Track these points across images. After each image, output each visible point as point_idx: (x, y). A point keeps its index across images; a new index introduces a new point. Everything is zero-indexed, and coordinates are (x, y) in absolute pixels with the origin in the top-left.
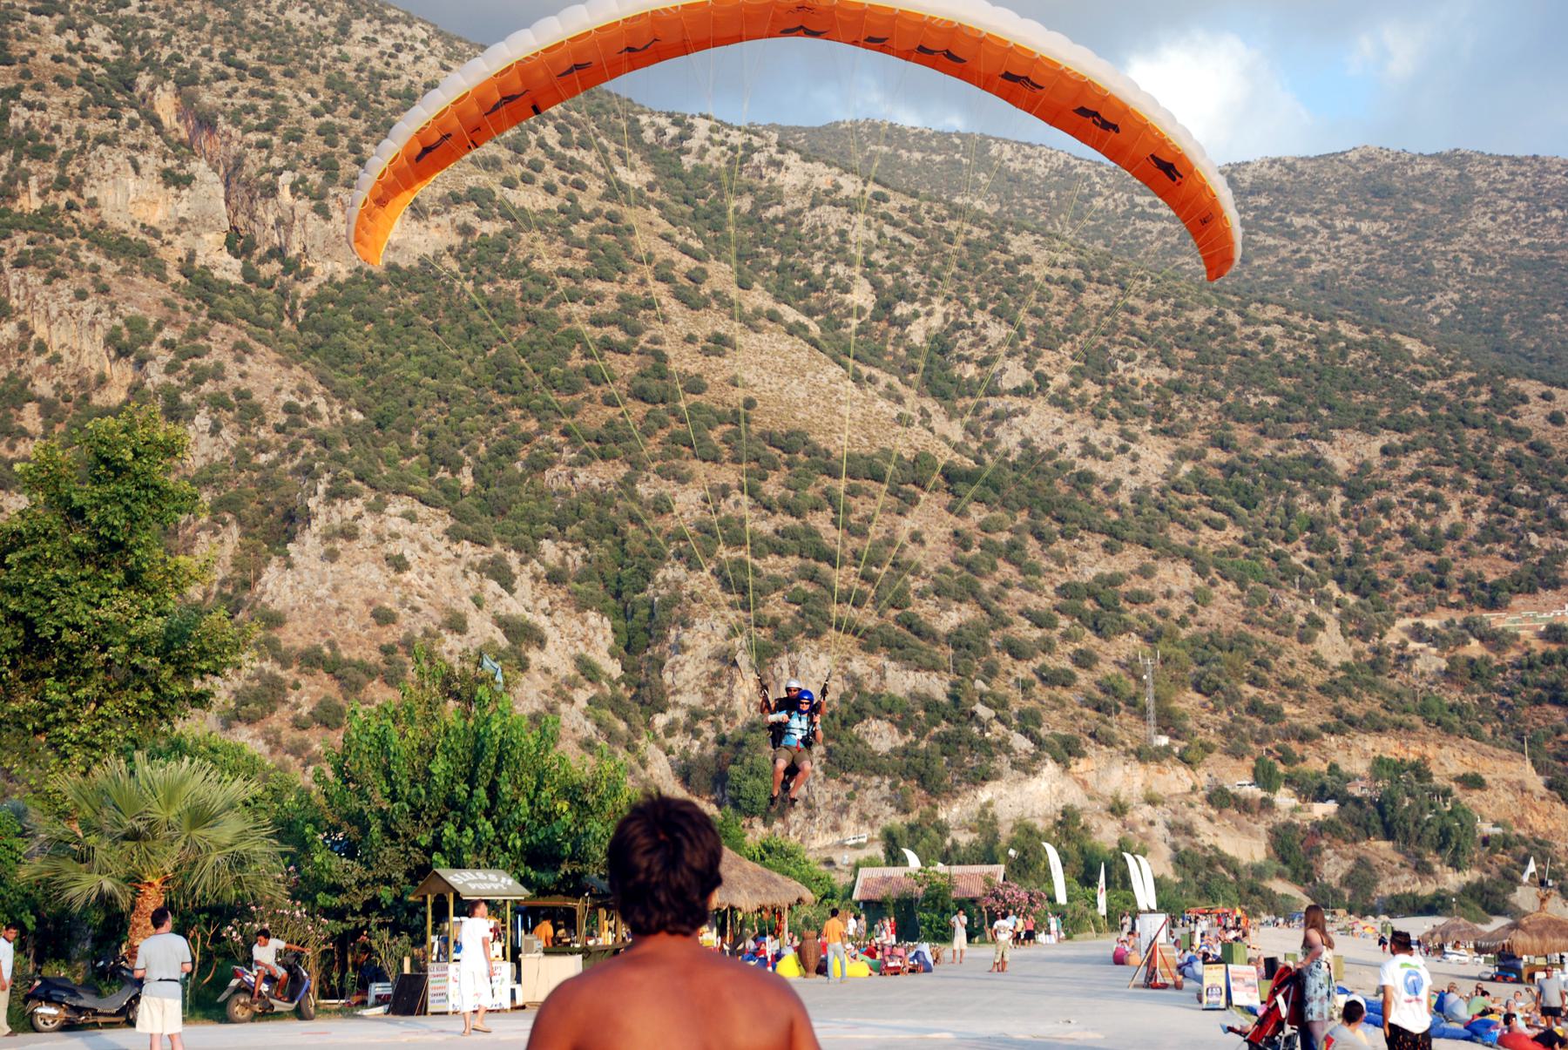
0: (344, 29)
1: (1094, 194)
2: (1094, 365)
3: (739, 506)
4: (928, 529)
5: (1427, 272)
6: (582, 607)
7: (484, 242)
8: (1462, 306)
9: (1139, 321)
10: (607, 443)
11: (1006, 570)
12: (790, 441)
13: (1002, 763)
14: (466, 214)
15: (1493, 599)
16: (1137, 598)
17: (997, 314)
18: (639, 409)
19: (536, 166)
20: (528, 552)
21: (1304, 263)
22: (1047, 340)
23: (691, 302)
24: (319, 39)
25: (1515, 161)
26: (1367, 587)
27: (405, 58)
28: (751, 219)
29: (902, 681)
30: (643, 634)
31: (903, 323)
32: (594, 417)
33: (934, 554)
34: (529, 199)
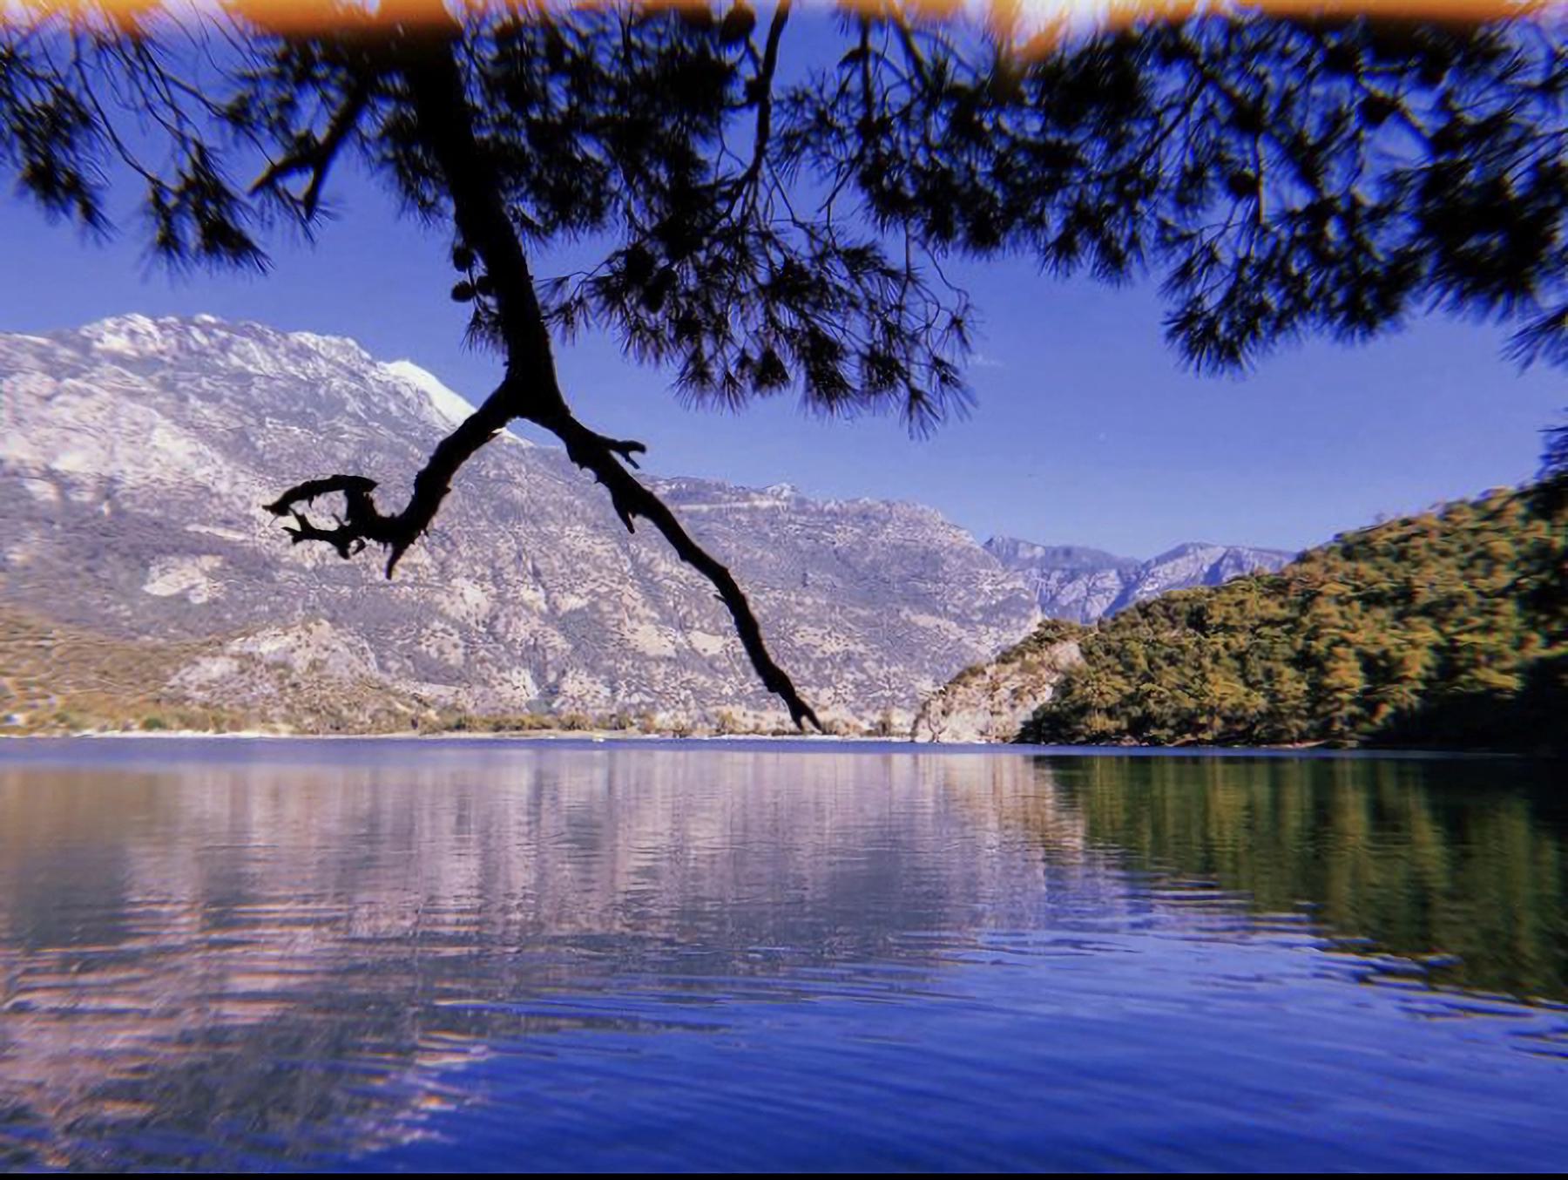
10: (611, 656)
12: (643, 653)
22: (706, 616)
29: (648, 699)
30: (614, 691)
32: (611, 650)
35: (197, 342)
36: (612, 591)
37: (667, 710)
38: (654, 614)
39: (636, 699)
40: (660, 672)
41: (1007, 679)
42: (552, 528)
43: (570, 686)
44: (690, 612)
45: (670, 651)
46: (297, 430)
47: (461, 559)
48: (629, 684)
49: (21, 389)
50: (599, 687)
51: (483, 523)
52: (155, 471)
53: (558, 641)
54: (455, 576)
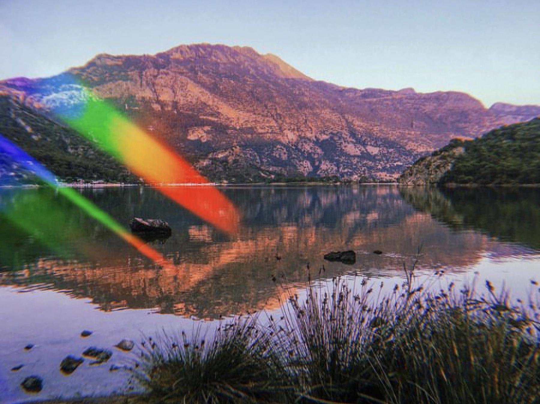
12: (349, 154)
15: (395, 162)
29: (350, 171)
30: (338, 168)
32: (338, 153)
34: (335, 132)
35: (201, 53)
37: (357, 174)
38: (354, 140)
39: (346, 170)
40: (355, 161)
41: (434, 162)
42: (318, 111)
43: (323, 167)
45: (359, 153)
46: (232, 82)
47: (286, 123)
49: (148, 74)
50: (333, 166)
51: (294, 111)
52: (189, 99)
53: (319, 151)
54: (285, 129)
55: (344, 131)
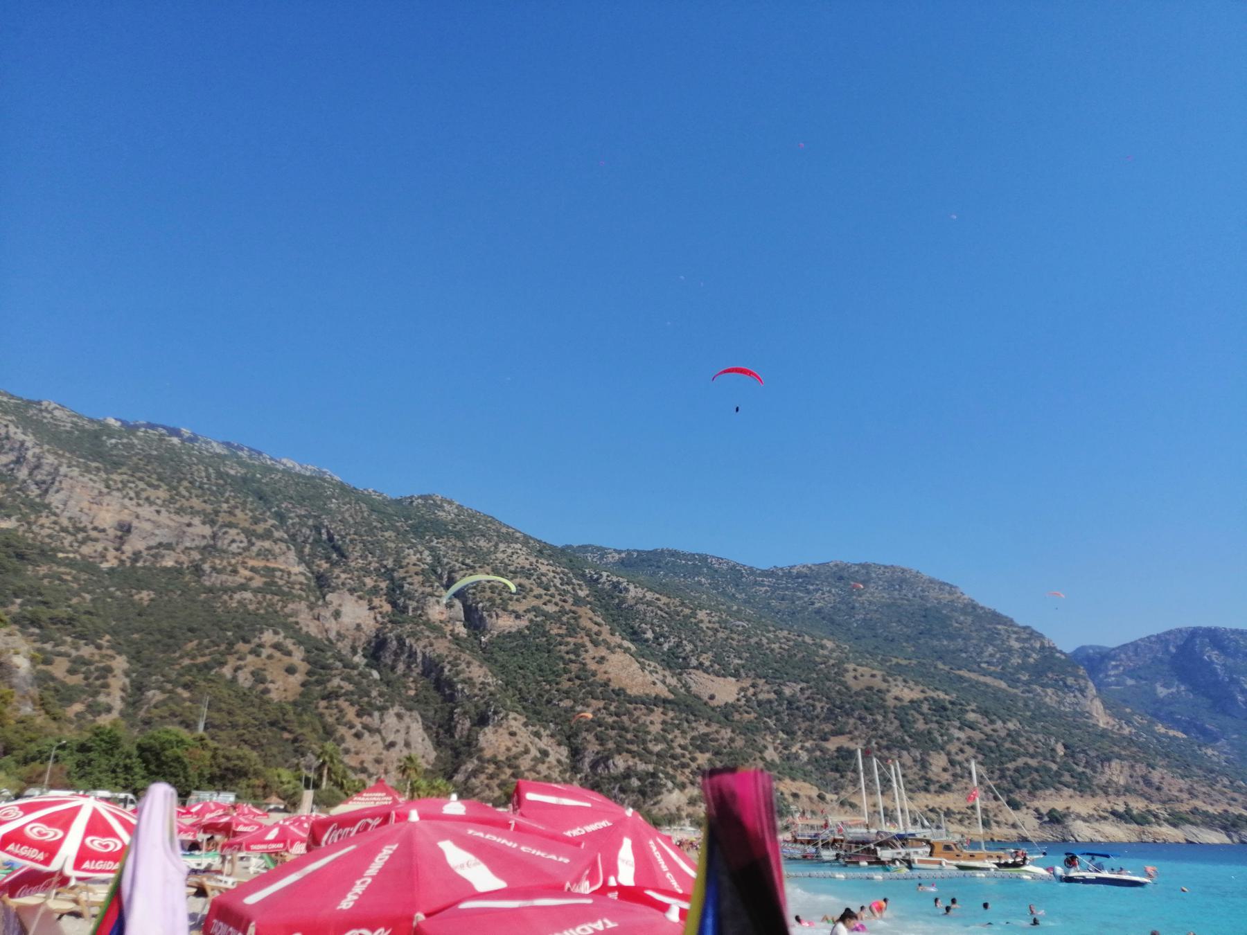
0: (496, 546)
1: (742, 576)
2: (717, 659)
3: (603, 714)
4: (655, 721)
5: (853, 608)
6: (559, 744)
7: (537, 625)
8: (864, 619)
9: (734, 643)
11: (677, 732)
12: (620, 692)
13: (664, 790)
14: (531, 615)
16: (712, 740)
17: (690, 641)
18: (578, 682)
19: (552, 596)
20: (545, 728)
21: (813, 604)
23: (596, 644)
24: (489, 553)
25: (886, 567)
26: (791, 733)
27: (515, 556)
28: (619, 606)
29: (641, 767)
31: (660, 644)
32: (566, 685)
33: (656, 729)
34: (551, 609)
36: (563, 612)
37: (682, 787)
38: (627, 644)
44: (679, 645)
48: (601, 740)
54: (334, 590)
55: (585, 611)
